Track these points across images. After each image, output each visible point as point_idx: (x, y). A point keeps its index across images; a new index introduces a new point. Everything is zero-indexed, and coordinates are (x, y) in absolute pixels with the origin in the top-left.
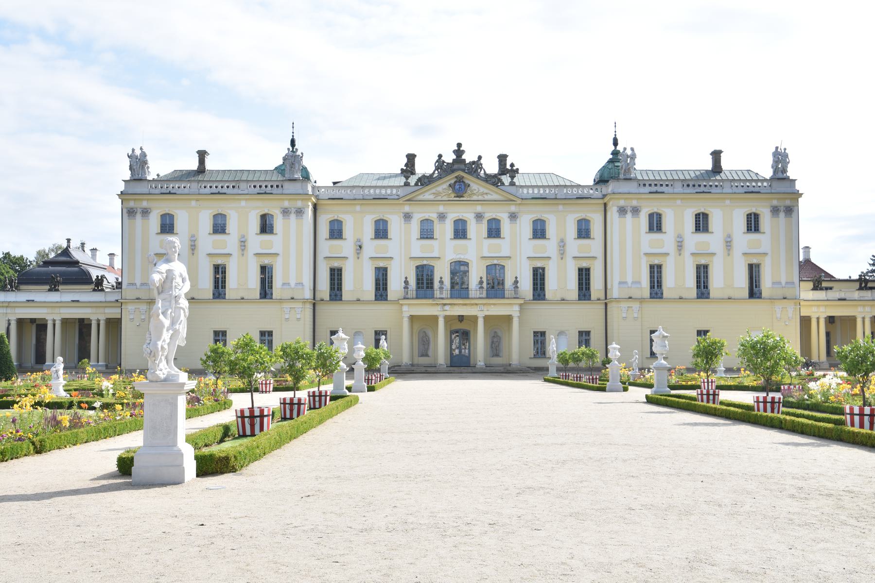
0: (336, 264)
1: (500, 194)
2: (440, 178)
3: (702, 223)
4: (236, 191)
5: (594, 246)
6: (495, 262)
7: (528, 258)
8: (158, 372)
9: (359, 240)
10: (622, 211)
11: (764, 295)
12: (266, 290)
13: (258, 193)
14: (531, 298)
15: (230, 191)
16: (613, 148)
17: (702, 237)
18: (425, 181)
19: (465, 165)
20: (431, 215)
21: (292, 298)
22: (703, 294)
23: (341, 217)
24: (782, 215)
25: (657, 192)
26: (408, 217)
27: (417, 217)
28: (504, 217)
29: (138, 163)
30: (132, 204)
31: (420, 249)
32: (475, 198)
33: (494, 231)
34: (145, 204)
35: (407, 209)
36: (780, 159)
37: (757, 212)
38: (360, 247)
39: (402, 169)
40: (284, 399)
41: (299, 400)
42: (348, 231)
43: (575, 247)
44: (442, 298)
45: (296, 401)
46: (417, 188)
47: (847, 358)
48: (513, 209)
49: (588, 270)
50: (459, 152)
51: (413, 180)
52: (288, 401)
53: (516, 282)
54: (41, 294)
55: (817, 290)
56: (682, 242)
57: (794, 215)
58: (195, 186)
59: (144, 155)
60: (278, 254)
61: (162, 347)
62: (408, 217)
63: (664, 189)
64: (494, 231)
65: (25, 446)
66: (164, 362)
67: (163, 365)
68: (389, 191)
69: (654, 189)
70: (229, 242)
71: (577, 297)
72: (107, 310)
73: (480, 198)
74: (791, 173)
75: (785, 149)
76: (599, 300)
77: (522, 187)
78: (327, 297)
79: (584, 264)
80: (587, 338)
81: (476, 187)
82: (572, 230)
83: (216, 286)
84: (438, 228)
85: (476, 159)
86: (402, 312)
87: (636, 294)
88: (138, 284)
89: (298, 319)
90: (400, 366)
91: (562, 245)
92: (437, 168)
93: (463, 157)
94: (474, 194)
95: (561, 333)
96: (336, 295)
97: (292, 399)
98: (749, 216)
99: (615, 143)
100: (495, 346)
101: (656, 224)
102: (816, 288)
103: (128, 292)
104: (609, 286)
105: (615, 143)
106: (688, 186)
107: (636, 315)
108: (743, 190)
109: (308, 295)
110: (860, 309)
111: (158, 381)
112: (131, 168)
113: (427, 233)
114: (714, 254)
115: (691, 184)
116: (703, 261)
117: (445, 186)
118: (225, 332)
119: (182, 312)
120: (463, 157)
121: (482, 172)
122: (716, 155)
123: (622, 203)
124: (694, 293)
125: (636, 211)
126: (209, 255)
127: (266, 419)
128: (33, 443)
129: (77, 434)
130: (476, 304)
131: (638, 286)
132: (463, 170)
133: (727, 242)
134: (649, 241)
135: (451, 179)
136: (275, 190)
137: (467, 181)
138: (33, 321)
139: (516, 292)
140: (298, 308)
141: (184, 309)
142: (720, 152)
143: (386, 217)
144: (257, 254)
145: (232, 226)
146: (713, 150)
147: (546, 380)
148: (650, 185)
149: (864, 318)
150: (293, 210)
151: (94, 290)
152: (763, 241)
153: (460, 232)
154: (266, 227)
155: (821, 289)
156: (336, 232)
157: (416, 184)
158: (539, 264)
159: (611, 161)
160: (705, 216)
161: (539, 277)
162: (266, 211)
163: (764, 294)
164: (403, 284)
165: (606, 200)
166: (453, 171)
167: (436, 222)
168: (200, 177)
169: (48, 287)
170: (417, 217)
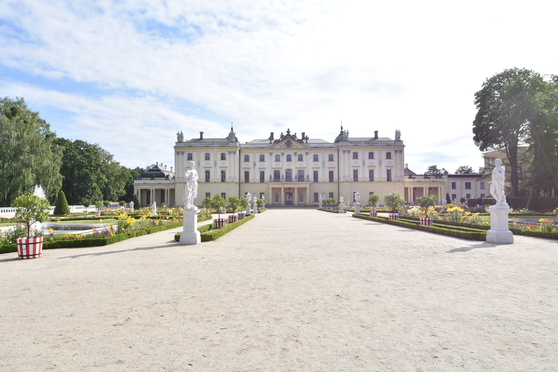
0: (247, 170)
2: (282, 140)
3: (371, 156)
4: (213, 145)
5: (334, 164)
6: (301, 169)
7: (312, 168)
8: (188, 207)
9: (255, 162)
10: (344, 152)
11: (392, 180)
12: (223, 179)
13: (220, 146)
14: (313, 181)
15: (211, 145)
16: (341, 130)
17: (371, 160)
18: (277, 142)
19: (291, 136)
20: (279, 153)
21: (232, 182)
22: (371, 180)
23: (248, 154)
24: (398, 153)
25: (356, 145)
26: (271, 154)
27: (274, 154)
28: (303, 153)
29: (180, 136)
30: (178, 150)
31: (275, 165)
32: (294, 147)
33: (300, 159)
34: (182, 150)
35: (271, 151)
36: (398, 134)
37: (390, 152)
38: (255, 164)
39: (269, 138)
40: (230, 216)
41: (235, 216)
42: (251, 159)
43: (328, 164)
44: (283, 182)
45: (234, 217)
46: (274, 144)
47: (421, 201)
48: (307, 151)
49: (332, 172)
50: (288, 132)
51: (273, 141)
52: (231, 217)
53: (308, 176)
54: (148, 181)
55: (410, 178)
56: (364, 162)
57: (402, 153)
58: (199, 144)
59: (182, 134)
61: (189, 198)
62: (271, 154)
63: (358, 144)
64: (300, 159)
65: (144, 231)
66: (190, 203)
67: (189, 204)
68: (265, 145)
69: (355, 144)
70: (211, 163)
71: (329, 181)
72: (170, 186)
73: (296, 147)
74: (401, 139)
75: (399, 131)
76: (336, 182)
77: (310, 144)
78: (244, 182)
79: (331, 170)
80: (332, 195)
81: (294, 143)
82: (327, 158)
83: (206, 178)
84: (281, 158)
85: (294, 134)
86: (269, 186)
87: (349, 180)
88: (180, 177)
89: (234, 189)
90: (268, 205)
91: (324, 163)
92: (281, 138)
93: (290, 134)
94: (294, 146)
95: (323, 193)
96: (247, 181)
97: (232, 216)
98: (387, 153)
99: (342, 128)
100: (301, 198)
101: (355, 156)
102: (410, 178)
103: (177, 180)
104: (340, 178)
105: (342, 128)
106: (367, 143)
107: (349, 187)
108: (385, 144)
109: (237, 181)
110: (425, 185)
111: (187, 210)
112: (178, 138)
113: (278, 160)
114: (375, 166)
115: (368, 142)
116: (372, 169)
117: (284, 143)
118: (210, 193)
119: (196, 186)
120: (290, 134)
121: (296, 138)
122: (376, 133)
123: (344, 149)
124: (368, 180)
125: (349, 152)
126: (204, 167)
127: (224, 223)
128: (147, 231)
129: (161, 227)
130: (295, 184)
132: (290, 138)
133: (380, 162)
134: (353, 162)
135: (286, 141)
136: (226, 145)
137: (291, 142)
138: (146, 190)
139: (308, 179)
141: (196, 186)
142: (377, 131)
143: (264, 154)
144: (220, 167)
145: (212, 157)
146: (375, 131)
147: (318, 209)
148: (354, 143)
149: (426, 188)
150: (232, 152)
151: (166, 179)
152: (392, 162)
153: (289, 159)
154: (223, 158)
155: (412, 178)
156: (247, 159)
157: (274, 143)
158: (316, 170)
159: (340, 135)
160: (372, 153)
161: (316, 174)
162: (223, 152)
163: (392, 180)
164: (270, 177)
165: (338, 148)
166: (286, 138)
167: (281, 156)
168: (201, 141)
169: (150, 178)
170: (274, 154)
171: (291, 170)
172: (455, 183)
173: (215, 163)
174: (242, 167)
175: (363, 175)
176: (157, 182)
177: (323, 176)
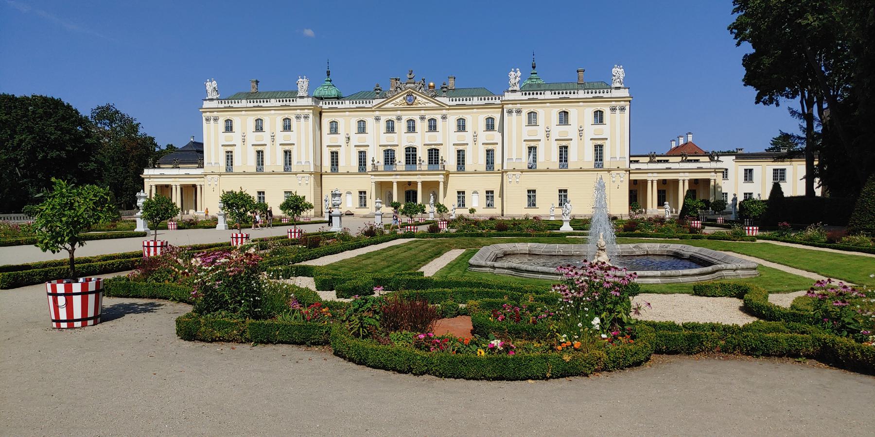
1: (437, 101)
3: (564, 117)
5: (496, 136)
6: (433, 147)
10: (510, 112)
23: (337, 119)
26: (377, 119)
31: (387, 139)
32: (420, 106)
33: (433, 127)
38: (349, 138)
48: (444, 112)
60: (294, 144)
62: (377, 119)
64: (433, 127)
73: (423, 105)
76: (499, 170)
78: (329, 171)
82: (482, 125)
124: (556, 166)
125: (519, 112)
131: (520, 161)
134: (528, 132)
137: (414, 95)
140: (307, 177)
145: (266, 126)
153: (411, 127)
154: (287, 127)
156: (334, 128)
160: (566, 113)
161: (461, 156)
167: (396, 121)
169: (171, 166)
171: (414, 149)
172: (751, 170)
173: (272, 136)
174: (325, 142)
175: (548, 156)
176: (182, 172)
177: (475, 159)
